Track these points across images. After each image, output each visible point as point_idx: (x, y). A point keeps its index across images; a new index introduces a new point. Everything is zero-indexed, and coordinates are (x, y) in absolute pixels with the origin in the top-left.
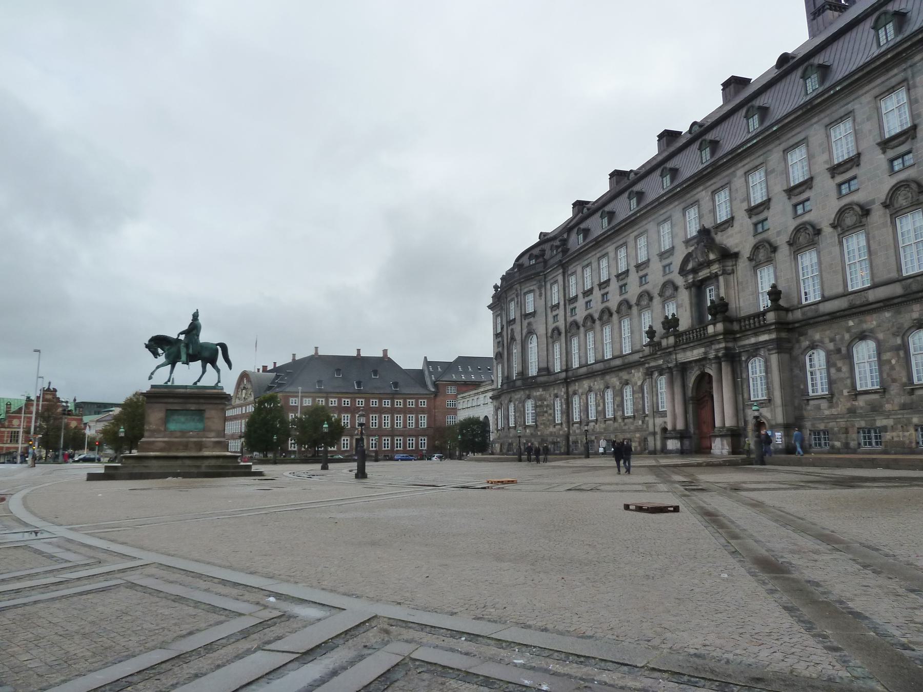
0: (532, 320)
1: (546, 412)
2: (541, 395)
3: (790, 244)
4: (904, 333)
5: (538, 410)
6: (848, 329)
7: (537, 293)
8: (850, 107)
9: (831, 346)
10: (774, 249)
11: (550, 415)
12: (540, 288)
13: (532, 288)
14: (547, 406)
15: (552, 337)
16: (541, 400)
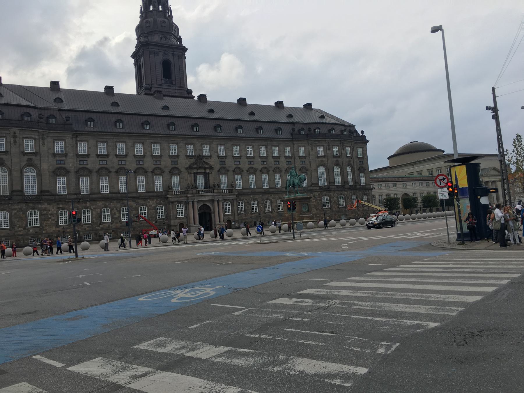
0: (33, 157)
1: (50, 218)
2: (46, 208)
3: (233, 171)
4: (263, 200)
5: (43, 217)
6: (251, 198)
7: (41, 142)
8: (253, 144)
9: (246, 201)
10: (228, 171)
11: (54, 220)
12: (43, 139)
13: (34, 136)
14: (51, 215)
15: (54, 172)
16: (46, 210)
